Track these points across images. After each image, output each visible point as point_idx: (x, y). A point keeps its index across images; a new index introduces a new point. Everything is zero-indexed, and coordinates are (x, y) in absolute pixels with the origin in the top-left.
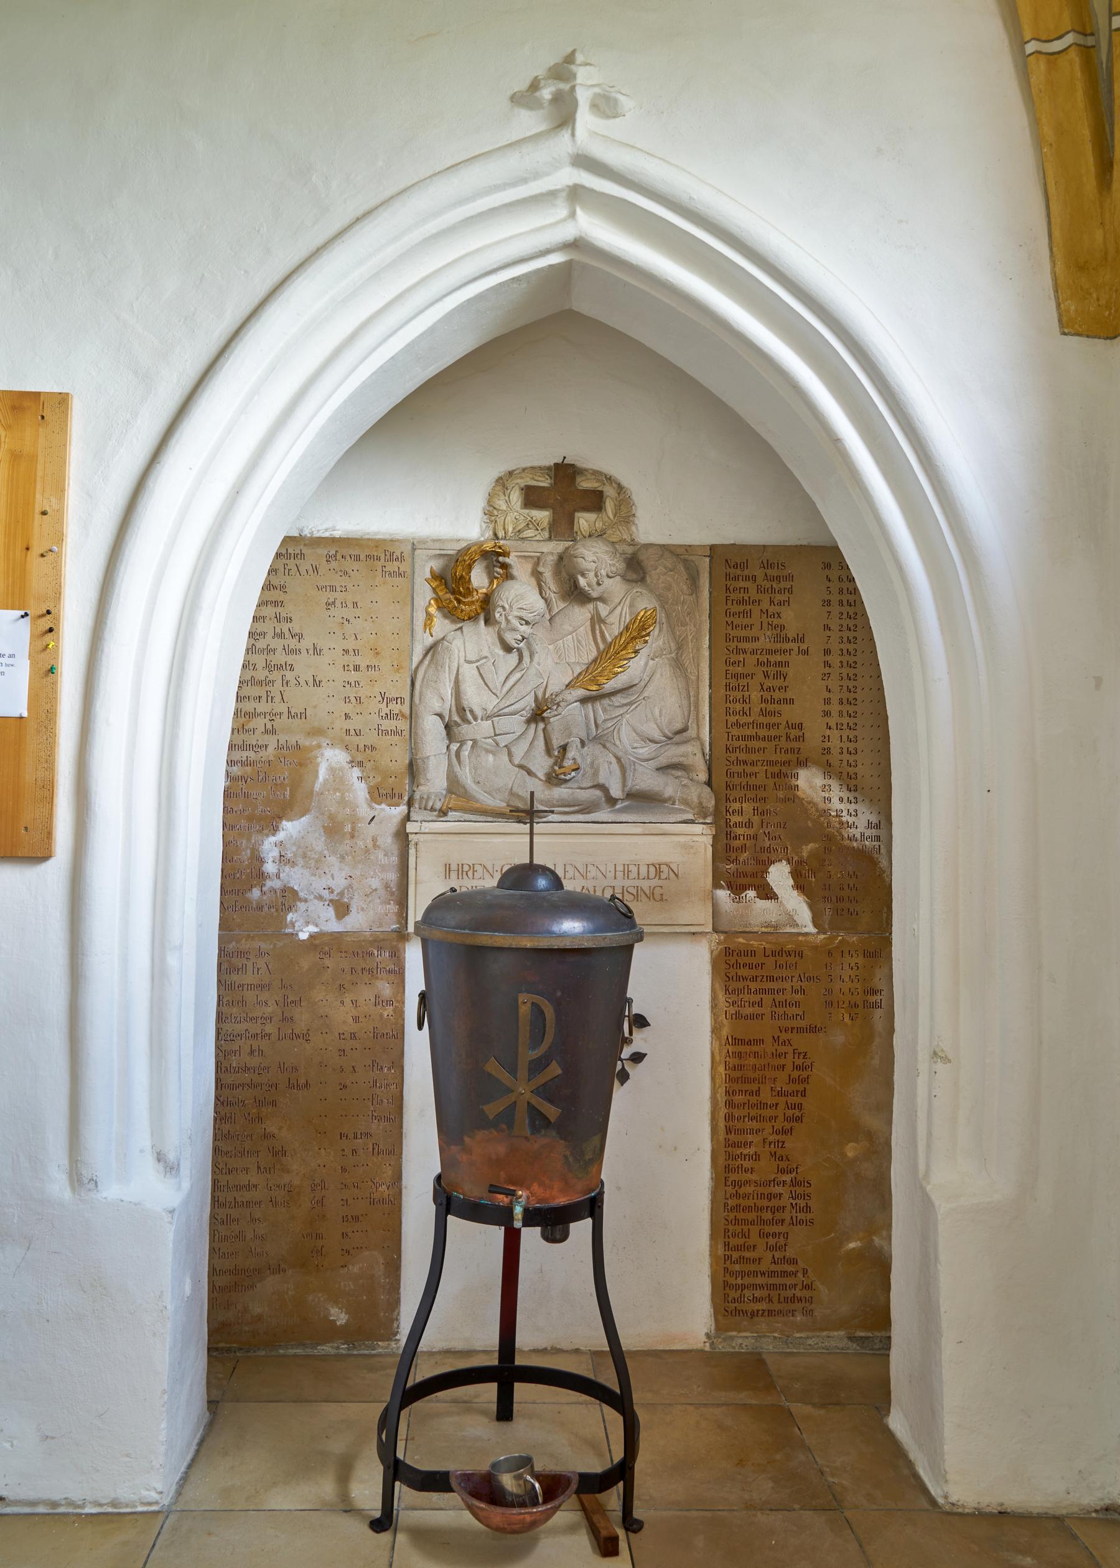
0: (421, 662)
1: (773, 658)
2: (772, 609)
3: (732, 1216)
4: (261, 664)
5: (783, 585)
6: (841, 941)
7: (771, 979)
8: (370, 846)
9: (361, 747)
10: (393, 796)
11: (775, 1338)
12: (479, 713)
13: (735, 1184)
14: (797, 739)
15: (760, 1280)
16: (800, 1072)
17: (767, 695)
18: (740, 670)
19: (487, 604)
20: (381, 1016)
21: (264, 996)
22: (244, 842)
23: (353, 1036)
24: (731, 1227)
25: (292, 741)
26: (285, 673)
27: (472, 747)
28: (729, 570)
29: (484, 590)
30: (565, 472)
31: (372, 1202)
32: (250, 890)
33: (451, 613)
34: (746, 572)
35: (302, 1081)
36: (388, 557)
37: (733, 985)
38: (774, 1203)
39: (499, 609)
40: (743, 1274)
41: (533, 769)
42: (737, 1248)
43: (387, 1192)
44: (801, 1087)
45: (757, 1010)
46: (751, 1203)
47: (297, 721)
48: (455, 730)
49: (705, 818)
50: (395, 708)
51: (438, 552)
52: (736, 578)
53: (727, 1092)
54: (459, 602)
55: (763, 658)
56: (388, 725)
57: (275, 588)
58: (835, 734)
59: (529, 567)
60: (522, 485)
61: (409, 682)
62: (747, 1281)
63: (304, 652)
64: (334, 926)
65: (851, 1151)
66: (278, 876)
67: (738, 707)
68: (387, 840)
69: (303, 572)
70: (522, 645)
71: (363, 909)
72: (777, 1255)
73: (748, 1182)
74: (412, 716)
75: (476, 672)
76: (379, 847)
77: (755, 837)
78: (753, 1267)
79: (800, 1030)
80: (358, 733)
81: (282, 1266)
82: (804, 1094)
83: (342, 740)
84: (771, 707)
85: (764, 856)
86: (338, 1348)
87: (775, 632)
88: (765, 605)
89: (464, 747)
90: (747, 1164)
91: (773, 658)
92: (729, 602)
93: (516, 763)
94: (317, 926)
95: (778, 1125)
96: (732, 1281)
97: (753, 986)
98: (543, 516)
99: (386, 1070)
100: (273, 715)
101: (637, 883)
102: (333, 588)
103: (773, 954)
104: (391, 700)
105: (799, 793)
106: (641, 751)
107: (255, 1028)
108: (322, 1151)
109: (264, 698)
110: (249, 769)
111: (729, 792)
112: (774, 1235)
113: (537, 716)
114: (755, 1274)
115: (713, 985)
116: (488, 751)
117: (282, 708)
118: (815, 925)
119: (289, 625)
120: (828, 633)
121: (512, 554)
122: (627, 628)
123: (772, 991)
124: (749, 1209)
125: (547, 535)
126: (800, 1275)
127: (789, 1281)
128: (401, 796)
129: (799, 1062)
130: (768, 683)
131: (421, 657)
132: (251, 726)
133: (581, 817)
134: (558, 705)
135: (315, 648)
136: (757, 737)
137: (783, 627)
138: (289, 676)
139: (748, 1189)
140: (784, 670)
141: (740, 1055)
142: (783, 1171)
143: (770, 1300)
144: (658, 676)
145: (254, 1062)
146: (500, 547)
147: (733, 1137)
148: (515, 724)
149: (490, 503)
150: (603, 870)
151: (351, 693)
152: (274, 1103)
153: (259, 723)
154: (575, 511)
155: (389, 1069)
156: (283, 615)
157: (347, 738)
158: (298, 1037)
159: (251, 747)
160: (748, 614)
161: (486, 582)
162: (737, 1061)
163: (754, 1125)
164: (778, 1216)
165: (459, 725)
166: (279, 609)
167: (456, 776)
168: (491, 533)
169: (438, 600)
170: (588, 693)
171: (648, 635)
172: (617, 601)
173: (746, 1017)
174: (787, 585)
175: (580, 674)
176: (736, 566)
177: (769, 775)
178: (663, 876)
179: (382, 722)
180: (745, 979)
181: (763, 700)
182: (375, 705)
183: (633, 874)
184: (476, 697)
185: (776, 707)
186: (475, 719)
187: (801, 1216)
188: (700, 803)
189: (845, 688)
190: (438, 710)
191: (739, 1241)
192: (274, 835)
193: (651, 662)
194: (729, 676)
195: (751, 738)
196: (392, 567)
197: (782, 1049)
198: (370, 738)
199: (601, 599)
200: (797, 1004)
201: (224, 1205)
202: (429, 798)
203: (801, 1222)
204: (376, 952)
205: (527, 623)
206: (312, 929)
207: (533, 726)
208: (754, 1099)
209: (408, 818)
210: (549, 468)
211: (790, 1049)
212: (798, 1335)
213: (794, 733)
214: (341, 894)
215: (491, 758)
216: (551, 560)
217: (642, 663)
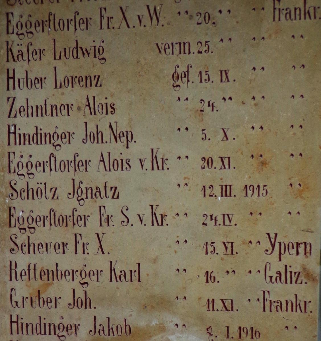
25: (118, 320)
47: (125, 286)
56: (281, 292)
63: (135, 164)
69: (133, 20)
80: (228, 307)
83: (201, 318)
100: (87, 275)
102: (184, 48)
104: (287, 248)
109: (71, 247)
117: (100, 263)
132: (51, 292)
135: (154, 158)
138: (112, 206)
151: (217, 235)
153: (64, 289)
157: (211, 314)
166: (93, 91)
179: (269, 287)
182: (258, 257)
198: (249, 315)
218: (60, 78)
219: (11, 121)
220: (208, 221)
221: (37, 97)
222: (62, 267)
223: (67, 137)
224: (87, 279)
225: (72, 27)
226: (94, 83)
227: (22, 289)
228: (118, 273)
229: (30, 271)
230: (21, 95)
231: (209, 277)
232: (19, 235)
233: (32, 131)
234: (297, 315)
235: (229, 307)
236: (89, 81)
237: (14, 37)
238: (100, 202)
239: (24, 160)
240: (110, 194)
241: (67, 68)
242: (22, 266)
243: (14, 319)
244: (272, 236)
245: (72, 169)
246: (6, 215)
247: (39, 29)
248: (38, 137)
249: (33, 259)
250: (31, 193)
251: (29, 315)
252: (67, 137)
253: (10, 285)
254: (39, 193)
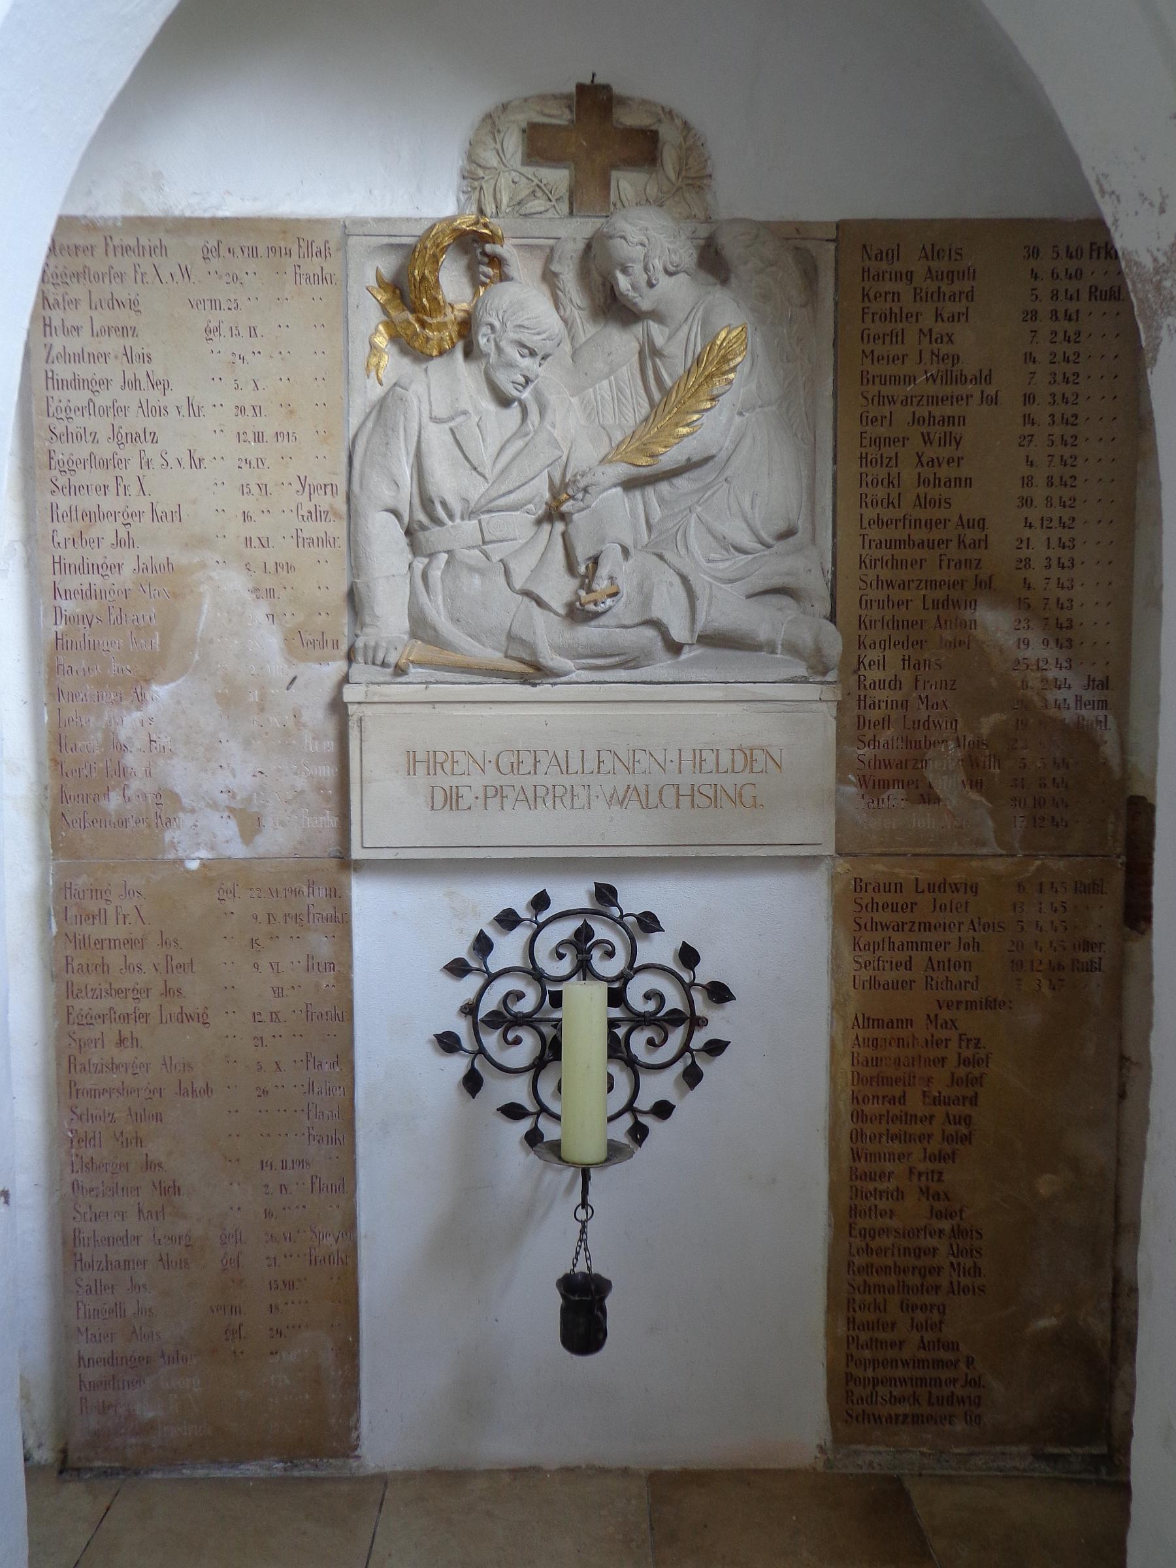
0: (363, 424)
1: (938, 411)
2: (939, 328)
3: (859, 1280)
4: (104, 433)
5: (957, 287)
6: (1038, 869)
7: (927, 927)
8: (290, 722)
9: (271, 567)
10: (323, 644)
11: (922, 1454)
12: (457, 507)
13: (863, 1233)
14: (976, 544)
15: (901, 1372)
16: (970, 1069)
17: (928, 472)
18: (883, 431)
19: (467, 328)
20: (317, 986)
21: (135, 957)
22: (92, 719)
23: (275, 1016)
24: (858, 1297)
25: (160, 559)
26: (144, 446)
27: (448, 563)
28: (867, 263)
29: (465, 306)
30: (594, 100)
31: (313, 1261)
32: (107, 795)
33: (410, 346)
34: (898, 266)
35: (200, 1084)
36: (304, 249)
37: (867, 937)
38: (925, 1261)
39: (485, 330)
40: (875, 1363)
41: (545, 597)
42: (867, 1326)
43: (334, 1248)
44: (969, 1092)
45: (903, 974)
46: (889, 1261)
48: (421, 535)
49: (824, 674)
50: (324, 501)
51: (386, 240)
52: (879, 277)
53: (855, 1099)
54: (423, 324)
55: (923, 412)
56: (312, 529)
57: (121, 304)
58: (1038, 536)
59: (537, 267)
60: (524, 125)
61: (345, 460)
62: (881, 1373)
63: (173, 411)
64: (237, 850)
65: (1046, 1185)
66: (148, 773)
67: (881, 492)
68: (316, 715)
69: (166, 277)
70: (526, 395)
71: (283, 824)
72: (929, 1336)
73: (884, 1231)
74: (352, 514)
75: (449, 438)
76: (304, 725)
77: (905, 704)
78: (891, 1354)
79: (971, 1005)
80: (264, 544)
81: (182, 1352)
82: (974, 1101)
84: (933, 493)
85: (919, 735)
86: (269, 1468)
87: (942, 367)
88: (927, 321)
89: (435, 563)
90: (883, 1204)
91: (938, 411)
92: (868, 318)
93: (518, 584)
94: (212, 848)
95: (934, 1147)
96: (859, 1373)
97: (898, 938)
98: (558, 177)
99: (326, 1067)
100: (129, 517)
101: (714, 778)
102: (215, 304)
103: (931, 888)
104: (316, 488)
105: (978, 633)
106: (721, 566)
107: (125, 1006)
108: (235, 1185)
110: (93, 604)
111: (863, 632)
112: (923, 1308)
113: (553, 514)
114: (894, 1363)
115: (834, 937)
116: (472, 569)
117: (143, 504)
118: (1000, 843)
119: (147, 367)
120: (1032, 367)
121: (508, 243)
122: (698, 361)
123: (927, 946)
124: (886, 1270)
125: (564, 208)
126: (962, 1365)
127: (944, 1374)
128: (336, 644)
129: (968, 1053)
130: (931, 452)
131: (363, 417)
132: (93, 533)
133: (623, 674)
134: (585, 490)
135: (190, 405)
136: (909, 543)
137: (956, 359)
138: (151, 450)
139: (886, 1241)
140: (956, 430)
141: (875, 1043)
142: (939, 1215)
143: (916, 1400)
144: (748, 441)
145: (126, 1055)
146: (486, 226)
147: (862, 1165)
148: (519, 525)
149: (471, 158)
150: (661, 760)
152: (158, 1117)
153: (106, 530)
154: (615, 166)
155: (332, 1066)
156: (137, 350)
157: (248, 551)
158: (190, 1018)
159: (96, 568)
160: (897, 337)
161: (468, 291)
162: (868, 1052)
163: (897, 1147)
164: (930, 1280)
165: (424, 528)
166: (129, 342)
167: (422, 611)
168: (474, 208)
169: (390, 325)
170: (634, 471)
171: (733, 370)
172: (681, 316)
173: (886, 986)
174: (966, 286)
175: (623, 442)
176: (880, 256)
177: (929, 604)
178: (757, 767)
179: (301, 525)
180: (885, 927)
181: (921, 481)
183: (710, 765)
184: (447, 480)
185: (943, 492)
186: (451, 516)
187: (966, 1281)
188: (818, 650)
189: (1057, 460)
190: (391, 503)
191: (871, 1316)
192: (139, 709)
193: (738, 419)
194: (866, 442)
195: (900, 543)
196: (313, 265)
197: (942, 1034)
199: (656, 315)
200: (967, 965)
201: (91, 1266)
202: (375, 649)
203: (965, 1290)
204: (305, 889)
205: (532, 353)
206: (204, 854)
207: (546, 527)
208: (896, 1110)
209: (346, 680)
210: (567, 97)
211: (953, 1034)
212: (957, 1451)
213: (971, 535)
214: (248, 800)
215: (477, 580)
216: (572, 249)
217: (723, 418)
218: (96, 328)
219: (48, 367)
220: (243, 465)
221: (74, 344)
222: (104, 509)
223: (106, 383)
224: (129, 520)
225: (107, 280)
226: (130, 333)
227: (64, 530)
228: (159, 514)
229: (72, 512)
230: (58, 342)
231: (246, 516)
232: (59, 476)
233: (70, 377)
234: (327, 551)
235: (265, 544)
236: (124, 331)
237: (50, 287)
238: (139, 446)
239: (63, 405)
240: (149, 438)
241: (103, 318)
242: (63, 507)
243: (57, 560)
244: (302, 478)
245: (111, 414)
246: (46, 458)
247: (74, 280)
248: (76, 383)
249: (74, 500)
250: (69, 436)
251: (72, 555)
252: (106, 383)
253: (51, 526)
254: (79, 437)
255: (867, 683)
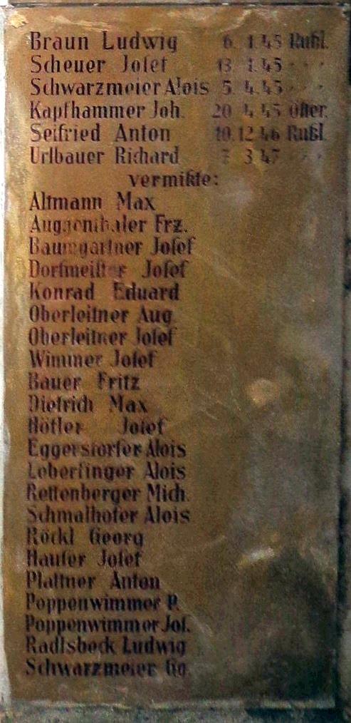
3: (41, 506)
7: (117, 89)
11: (117, 710)
13: (45, 451)
15: (91, 615)
16: (169, 256)
24: (40, 526)
37: (46, 101)
38: (119, 483)
40: (60, 604)
42: (51, 560)
44: (169, 283)
45: (90, 145)
46: (76, 484)
53: (34, 292)
62: (67, 615)
65: (260, 392)
72: (123, 572)
73: (71, 448)
78: (79, 593)
79: (169, 181)
82: (174, 294)
90: (69, 417)
95: (127, 348)
96: (41, 615)
97: (83, 102)
103: (121, 43)
112: (117, 538)
114: (83, 604)
115: (8, 102)
123: (118, 111)
124: (73, 494)
126: (163, 606)
127: (143, 616)
129: (166, 237)
139: (71, 460)
141: (57, 227)
142: (134, 429)
143: (109, 647)
147: (44, 371)
162: (49, 237)
163: (84, 349)
164: (125, 505)
173: (70, 159)
180: (67, 89)
187: (166, 506)
191: (57, 549)
197: (136, 215)
200: (165, 134)
203: (166, 516)
208: (82, 305)
211: (149, 216)
212: (158, 706)
255: (37, 646)
